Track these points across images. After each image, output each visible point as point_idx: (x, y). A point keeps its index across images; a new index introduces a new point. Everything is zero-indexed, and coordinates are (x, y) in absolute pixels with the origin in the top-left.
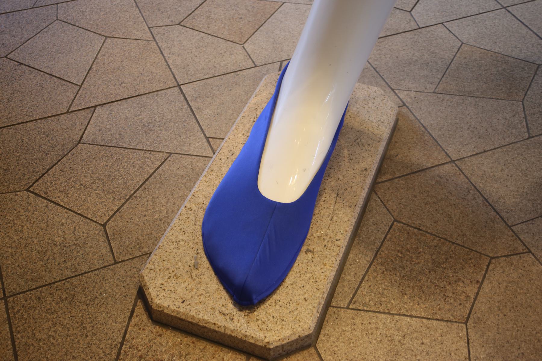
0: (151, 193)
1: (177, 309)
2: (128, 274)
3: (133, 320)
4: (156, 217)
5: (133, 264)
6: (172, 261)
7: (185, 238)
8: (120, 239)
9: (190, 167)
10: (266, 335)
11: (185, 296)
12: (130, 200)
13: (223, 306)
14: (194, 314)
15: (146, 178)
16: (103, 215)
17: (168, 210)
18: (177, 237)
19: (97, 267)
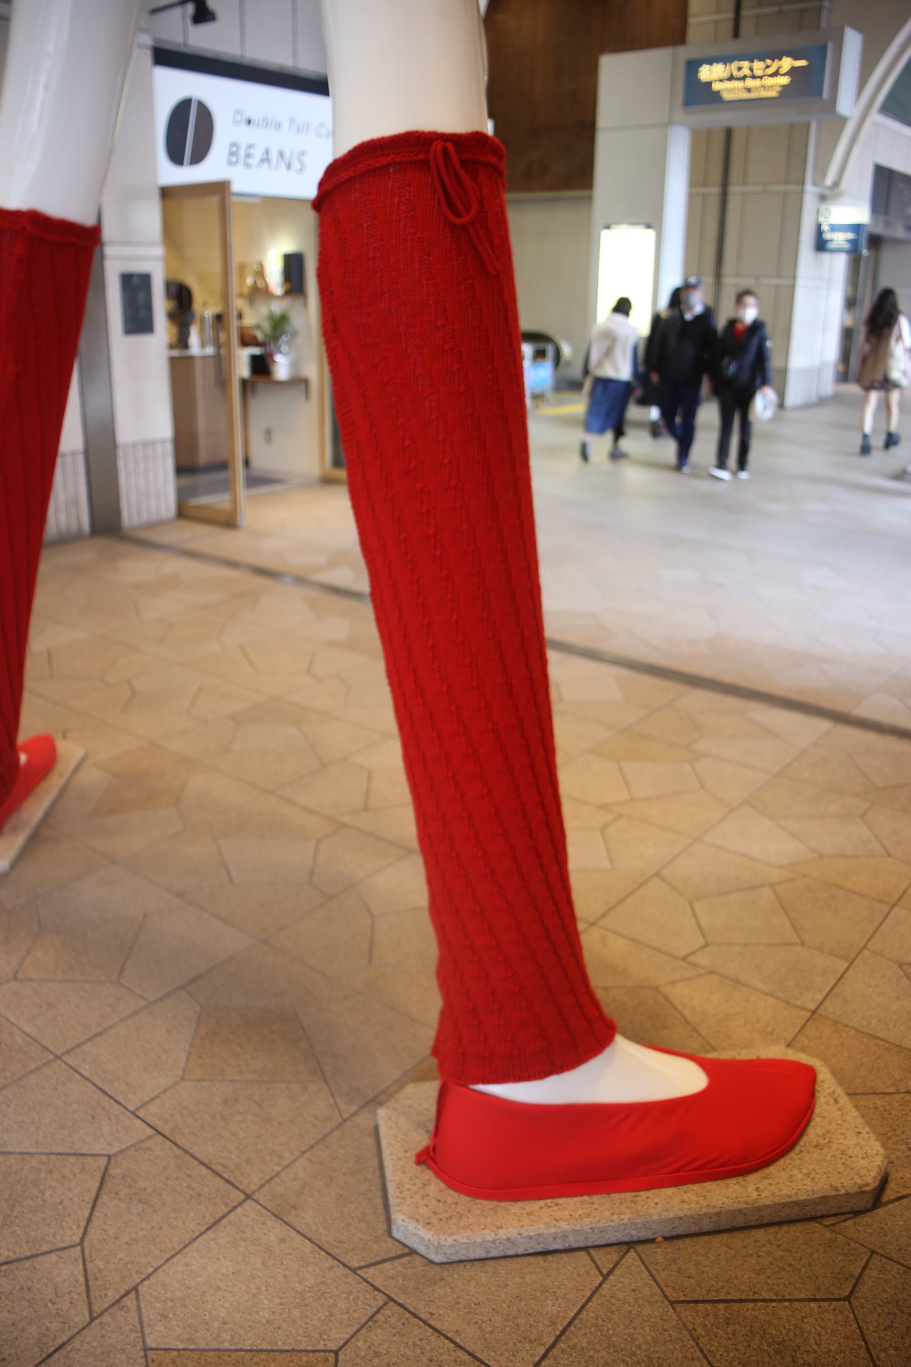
3: (904, 1193)
4: (781, 1253)
7: (796, 1172)
9: (673, 1266)
12: (787, 1297)
15: (738, 1305)
16: (837, 1312)
18: (802, 1180)
19: (896, 1266)
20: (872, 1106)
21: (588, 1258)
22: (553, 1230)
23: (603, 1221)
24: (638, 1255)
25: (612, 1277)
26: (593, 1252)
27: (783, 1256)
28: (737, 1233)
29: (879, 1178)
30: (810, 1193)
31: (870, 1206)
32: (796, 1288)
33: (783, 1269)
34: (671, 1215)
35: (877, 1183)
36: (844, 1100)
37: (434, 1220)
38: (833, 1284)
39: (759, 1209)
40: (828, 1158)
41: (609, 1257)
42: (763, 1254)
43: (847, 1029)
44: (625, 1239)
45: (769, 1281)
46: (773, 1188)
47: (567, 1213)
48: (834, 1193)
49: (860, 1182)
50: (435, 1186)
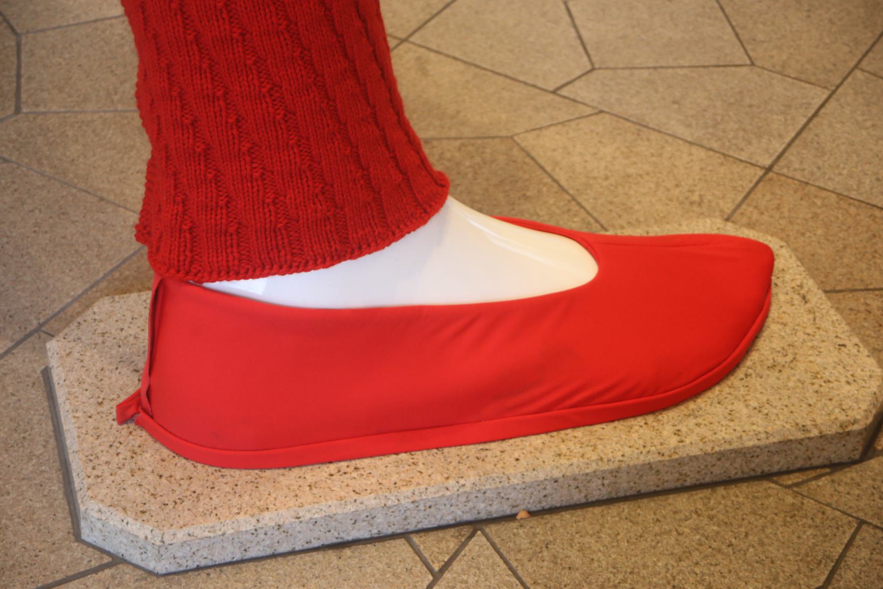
0: (675, 571)
1: (860, 344)
2: (857, 492)
4: (715, 528)
5: (835, 498)
6: (797, 395)
7: (739, 406)
8: (817, 548)
9: (545, 553)
10: (777, 247)
11: (832, 348)
13: (793, 305)
14: (843, 325)
17: (680, 520)
20: (862, 308)
21: (410, 549)
22: (351, 508)
23: (431, 490)
24: (488, 539)
25: (447, 575)
26: (416, 539)
27: (718, 533)
28: (645, 501)
29: (874, 412)
30: (763, 436)
31: (857, 455)
32: (740, 578)
33: (719, 551)
34: (542, 477)
35: (870, 419)
36: (817, 297)
37: (153, 506)
38: (799, 571)
39: (680, 462)
40: (791, 384)
41: (443, 545)
42: (687, 530)
43: (824, 194)
44: (467, 517)
45: (697, 570)
46: (702, 430)
47: (374, 480)
48: (800, 435)
49: (842, 417)
50: (153, 454)
